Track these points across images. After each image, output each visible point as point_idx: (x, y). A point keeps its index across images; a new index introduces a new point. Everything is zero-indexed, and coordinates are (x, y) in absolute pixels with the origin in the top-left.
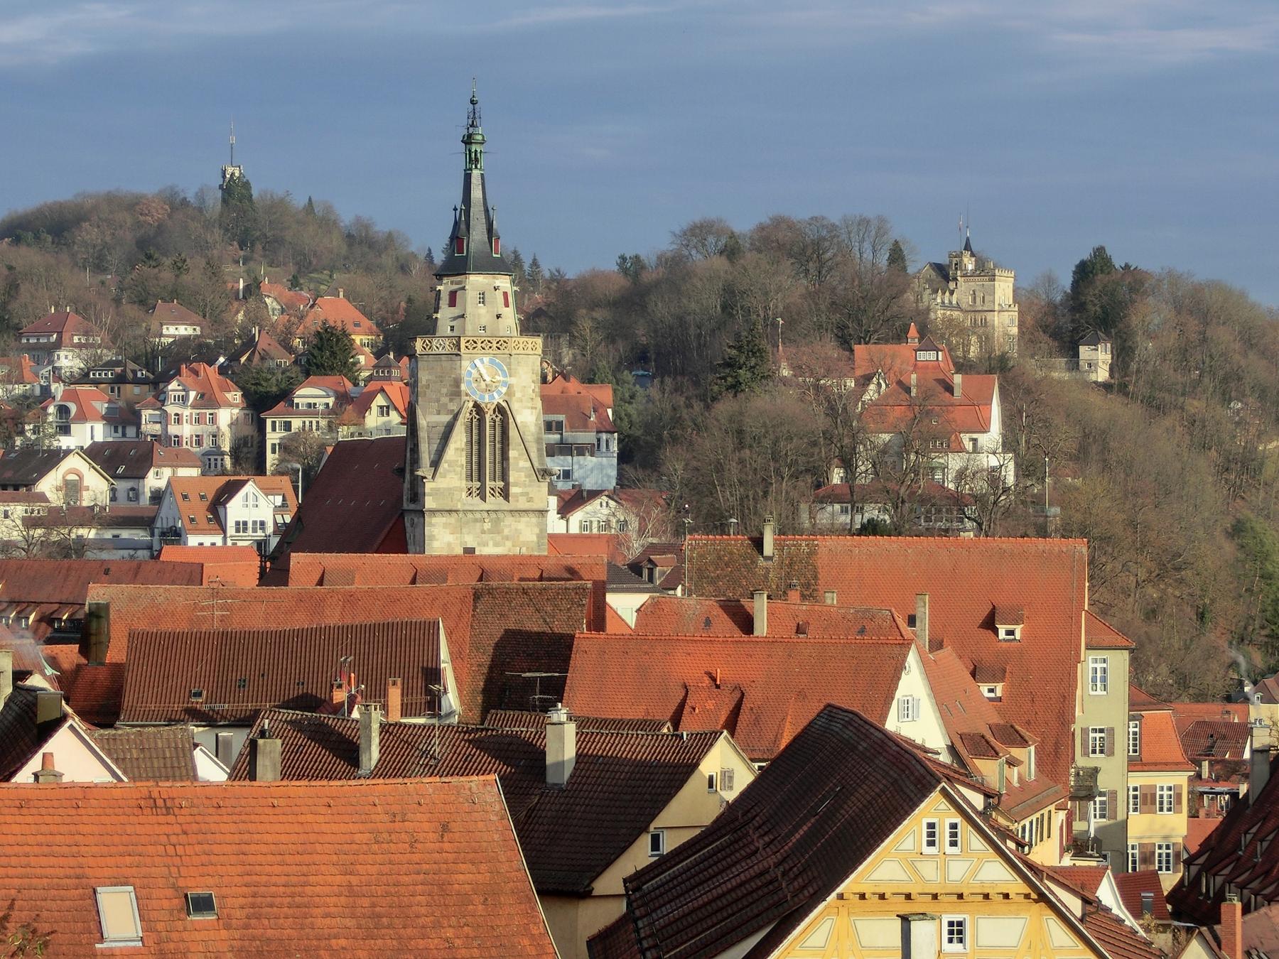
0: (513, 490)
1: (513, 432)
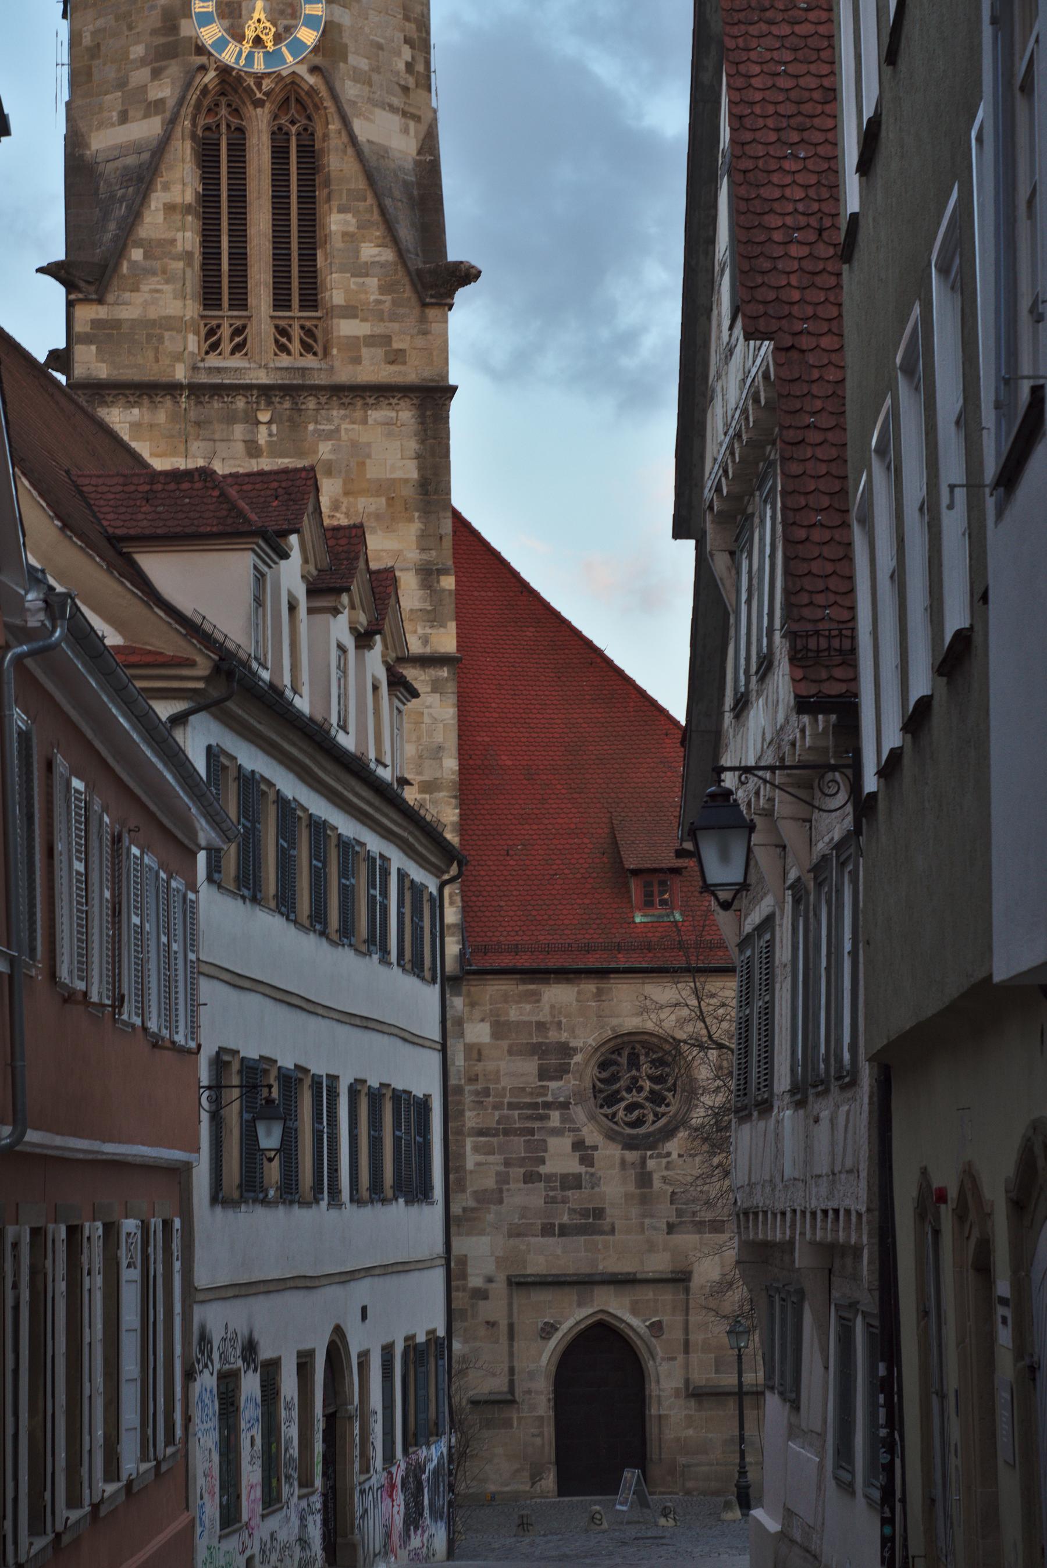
0: (347, 328)
1: (338, 163)
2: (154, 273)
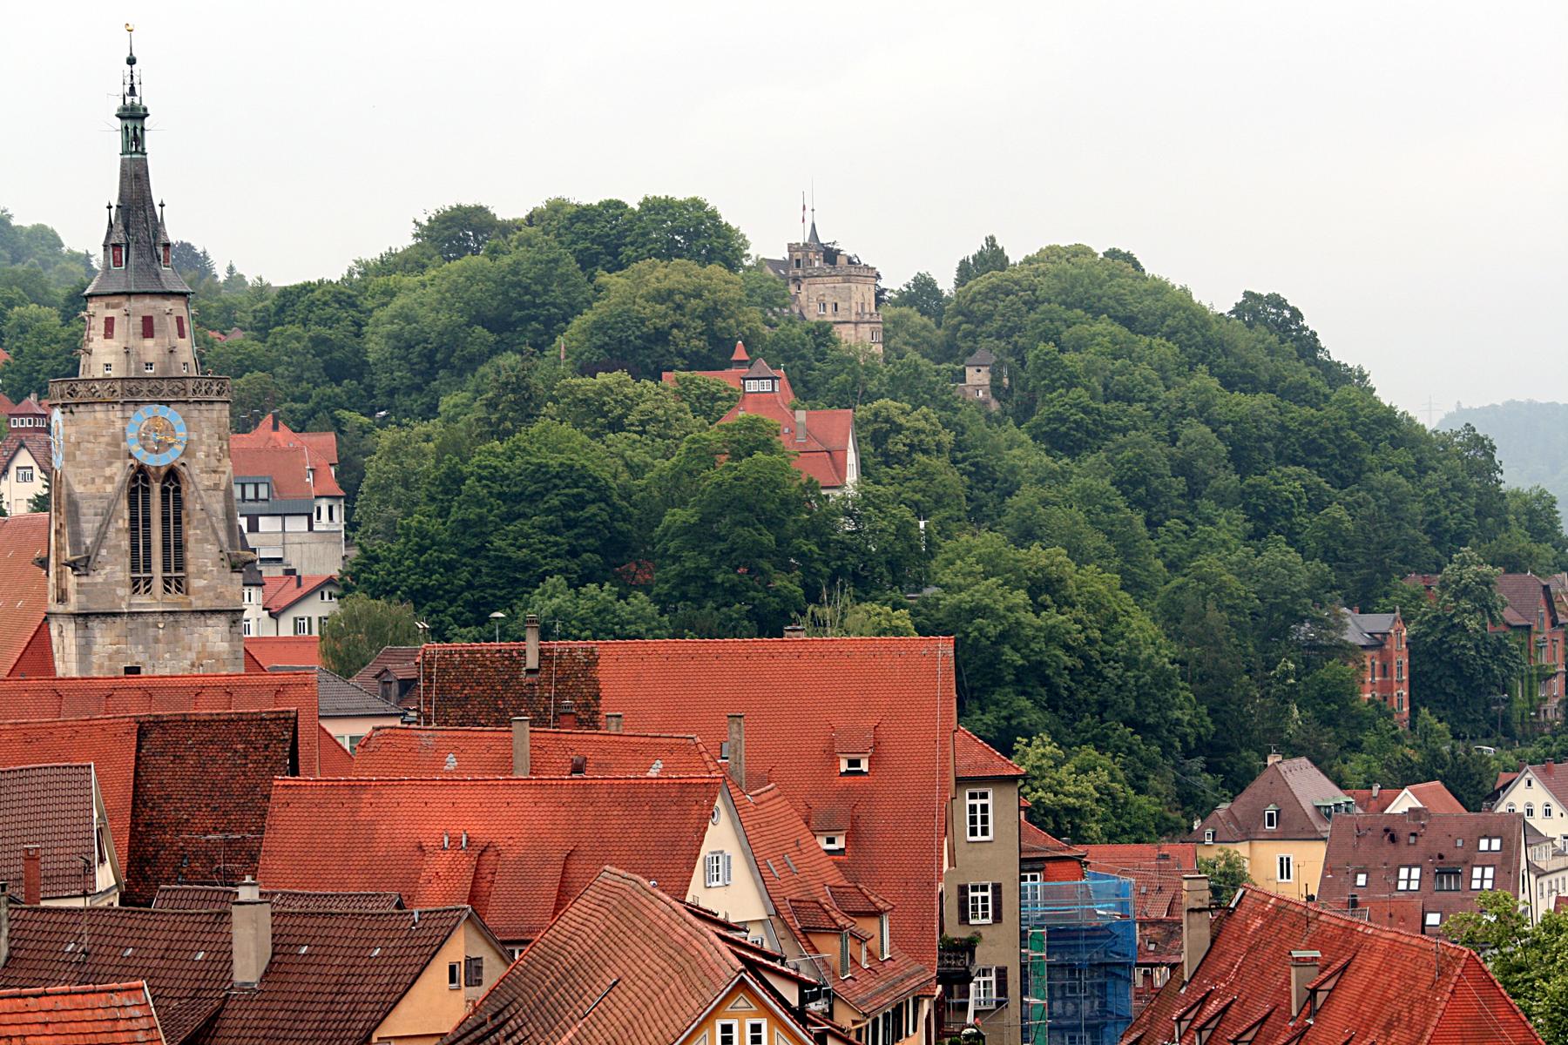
0: (196, 583)
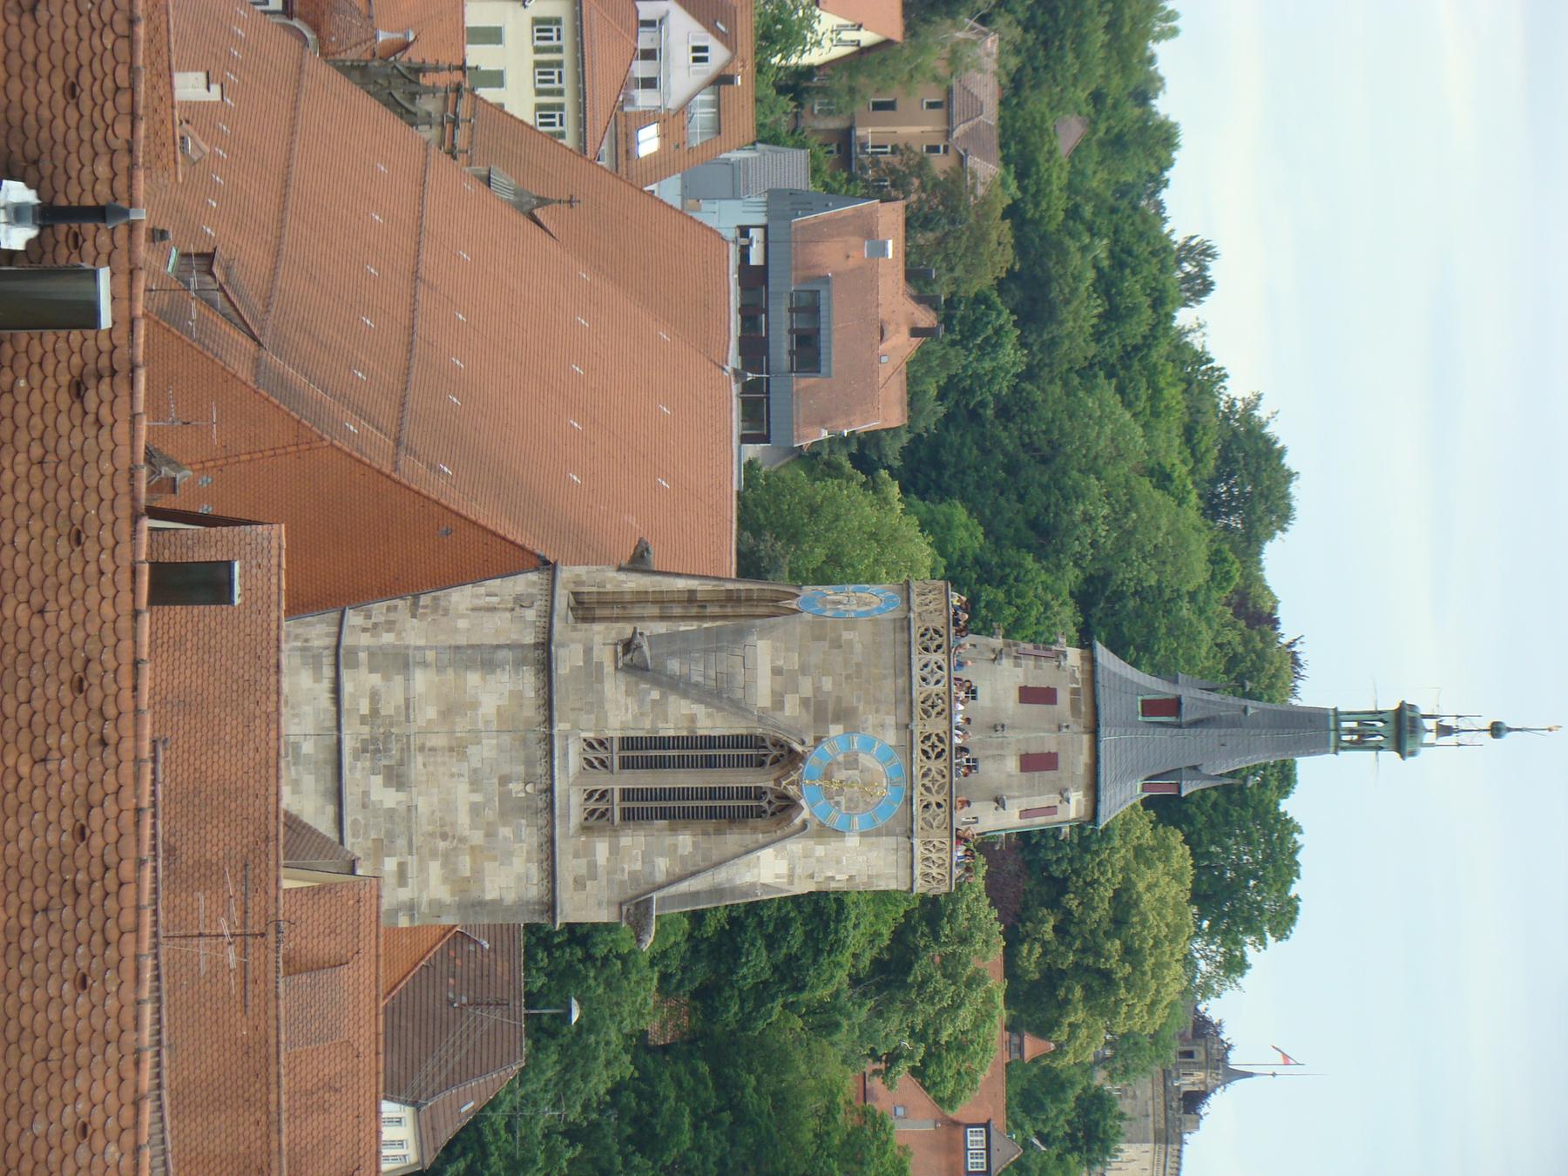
0: (602, 848)
1: (733, 839)
2: (640, 707)
